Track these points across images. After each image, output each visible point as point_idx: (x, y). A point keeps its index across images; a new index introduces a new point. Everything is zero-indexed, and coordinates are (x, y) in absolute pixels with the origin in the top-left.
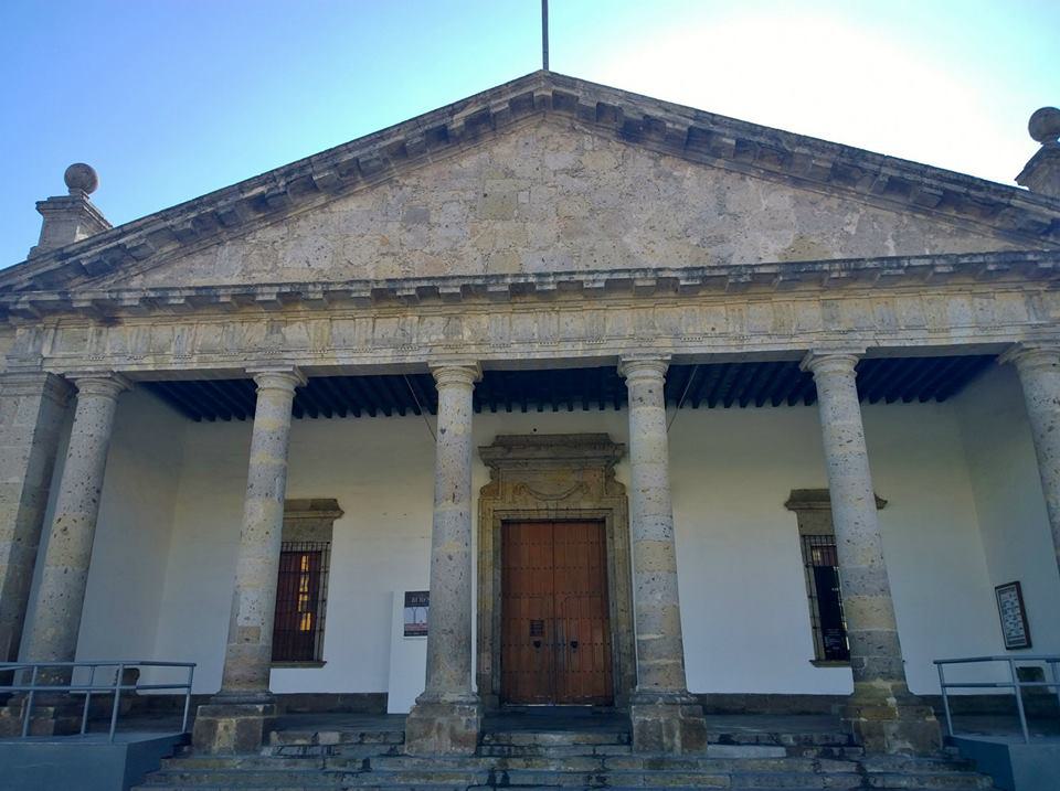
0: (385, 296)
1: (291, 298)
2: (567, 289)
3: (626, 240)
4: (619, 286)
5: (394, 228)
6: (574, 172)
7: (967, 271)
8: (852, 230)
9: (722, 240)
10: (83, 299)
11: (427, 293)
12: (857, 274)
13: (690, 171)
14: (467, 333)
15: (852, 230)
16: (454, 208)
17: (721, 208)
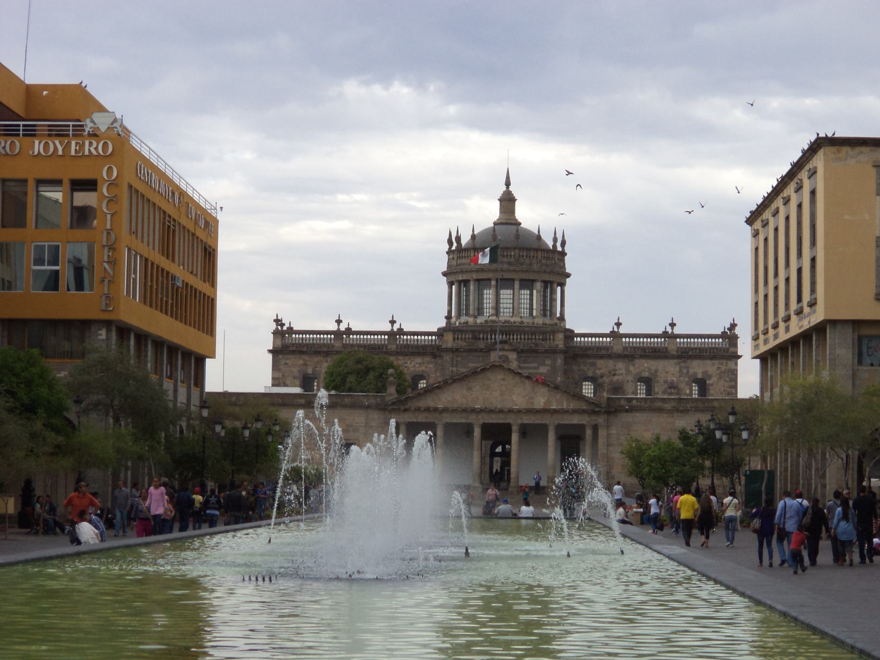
0: (464, 410)
1: (445, 410)
2: (501, 411)
3: (514, 397)
4: (511, 411)
5: (464, 391)
6: (503, 379)
7: (575, 411)
8: (558, 398)
9: (532, 398)
10: (402, 408)
11: (473, 411)
12: (555, 411)
13: (527, 381)
14: (480, 417)
15: (558, 398)
16: (478, 387)
17: (534, 391)
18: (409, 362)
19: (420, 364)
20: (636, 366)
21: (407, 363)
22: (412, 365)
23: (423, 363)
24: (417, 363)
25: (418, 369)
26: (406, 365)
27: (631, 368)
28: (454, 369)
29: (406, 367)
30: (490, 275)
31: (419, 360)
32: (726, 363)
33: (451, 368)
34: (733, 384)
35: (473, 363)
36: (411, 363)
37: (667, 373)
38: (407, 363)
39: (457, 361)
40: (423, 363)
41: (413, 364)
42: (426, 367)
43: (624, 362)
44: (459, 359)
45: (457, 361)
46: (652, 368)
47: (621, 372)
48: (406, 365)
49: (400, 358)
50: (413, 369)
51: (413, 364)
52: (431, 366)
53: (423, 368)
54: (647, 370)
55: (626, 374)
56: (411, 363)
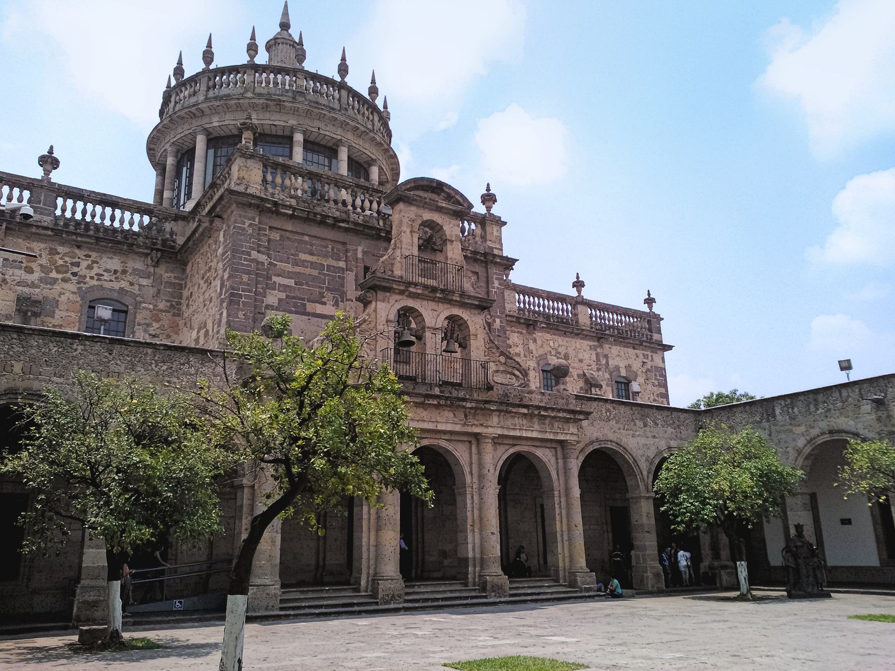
18: (84, 264)
19: (116, 272)
20: (539, 342)
21: (78, 265)
22: (93, 273)
23: (124, 272)
24: (106, 270)
25: (107, 285)
26: (75, 269)
27: (532, 346)
28: (262, 258)
29: (75, 274)
30: (292, 122)
31: (114, 263)
32: (652, 356)
33: (254, 254)
34: (663, 390)
35: (312, 254)
36: (90, 267)
37: (581, 361)
38: (78, 265)
39: (269, 241)
40: (124, 272)
41: (96, 270)
42: (132, 284)
43: (521, 333)
44: (275, 236)
45: (269, 241)
46: (560, 350)
47: (517, 350)
48: (75, 269)
49: (60, 249)
50: (95, 283)
51: (96, 270)
52: (144, 282)
53: (124, 284)
54: (553, 353)
55: (525, 356)
56: (90, 267)
